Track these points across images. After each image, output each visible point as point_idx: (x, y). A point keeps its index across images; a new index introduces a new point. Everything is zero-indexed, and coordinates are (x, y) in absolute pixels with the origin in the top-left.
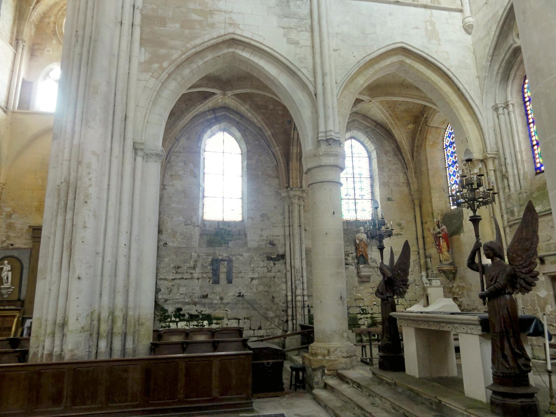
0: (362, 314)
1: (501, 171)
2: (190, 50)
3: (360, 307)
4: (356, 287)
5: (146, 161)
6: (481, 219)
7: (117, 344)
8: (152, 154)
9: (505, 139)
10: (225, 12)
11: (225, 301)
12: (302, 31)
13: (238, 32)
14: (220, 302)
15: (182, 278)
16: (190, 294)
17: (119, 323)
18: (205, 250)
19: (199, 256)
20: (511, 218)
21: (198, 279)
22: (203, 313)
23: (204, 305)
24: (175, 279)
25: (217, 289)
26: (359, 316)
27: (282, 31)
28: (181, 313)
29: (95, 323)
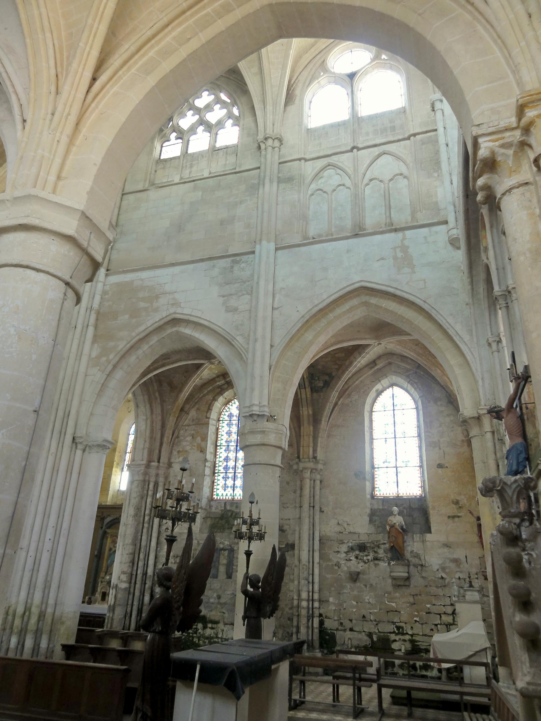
0: (397, 634)
2: (134, 338)
3: (394, 623)
4: (389, 593)
5: (89, 453)
6: (176, 540)
7: (29, 643)
8: (93, 445)
10: (169, 293)
11: (222, 601)
12: (243, 295)
13: (179, 310)
14: (217, 601)
17: (33, 620)
25: (215, 585)
26: (393, 637)
27: (221, 300)
29: (10, 618)
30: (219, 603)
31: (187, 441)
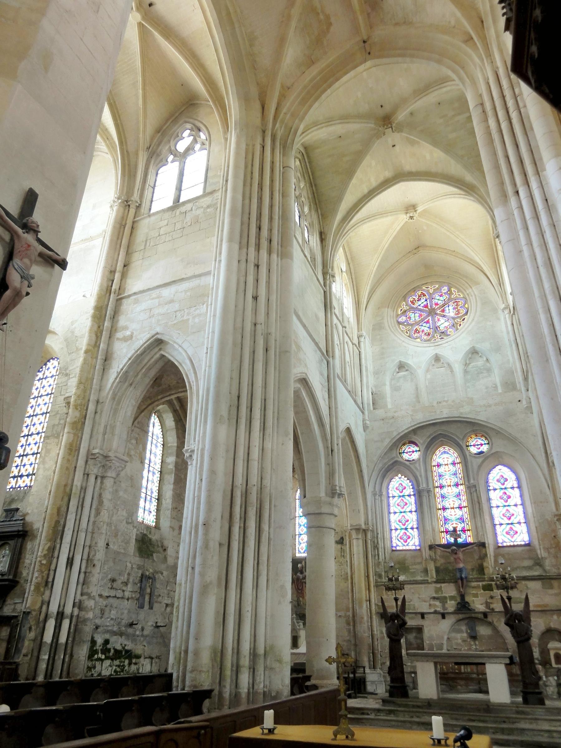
1: (374, 542)
9: (378, 520)
11: (145, 633)
15: (115, 597)
16: (119, 620)
18: (137, 560)
19: (132, 568)
20: (379, 580)
21: (128, 599)
22: (126, 648)
23: (128, 636)
24: (110, 596)
28: (108, 646)
30: (142, 636)
31: (132, 444)
